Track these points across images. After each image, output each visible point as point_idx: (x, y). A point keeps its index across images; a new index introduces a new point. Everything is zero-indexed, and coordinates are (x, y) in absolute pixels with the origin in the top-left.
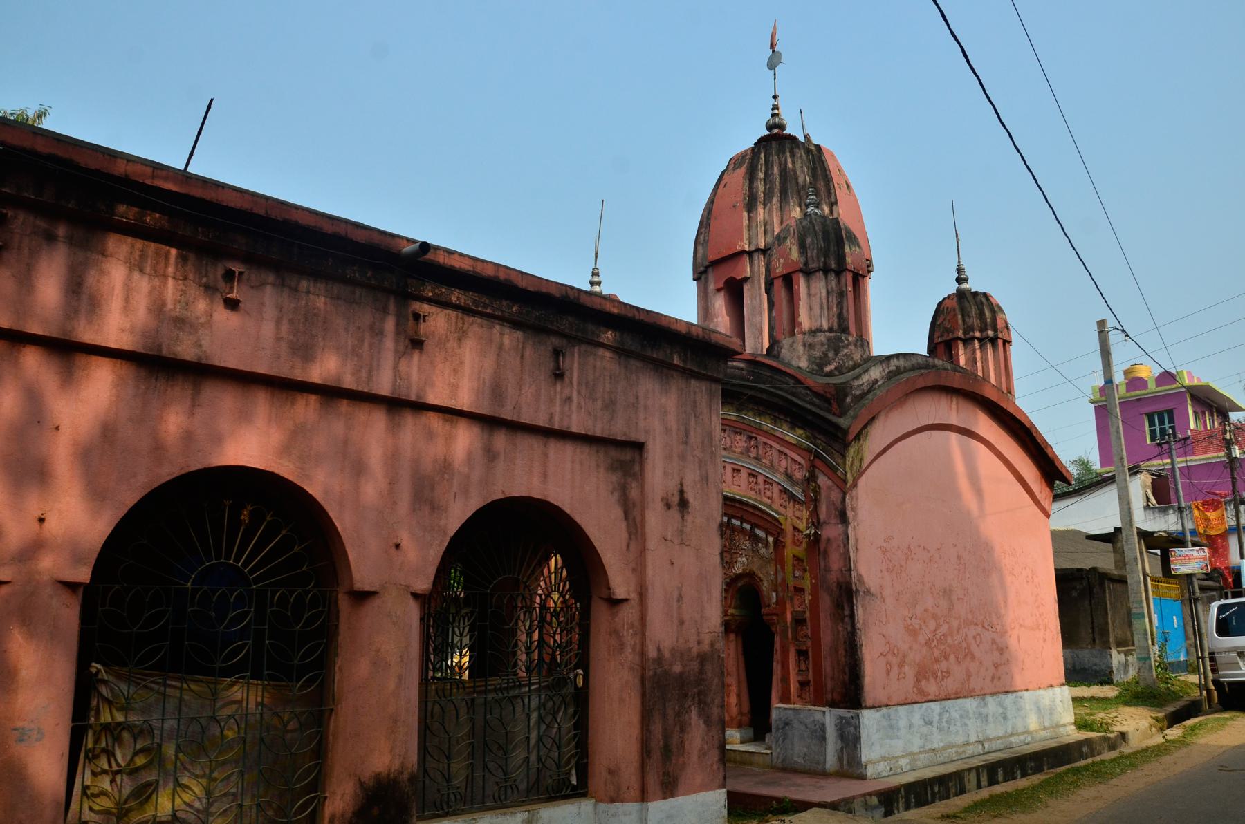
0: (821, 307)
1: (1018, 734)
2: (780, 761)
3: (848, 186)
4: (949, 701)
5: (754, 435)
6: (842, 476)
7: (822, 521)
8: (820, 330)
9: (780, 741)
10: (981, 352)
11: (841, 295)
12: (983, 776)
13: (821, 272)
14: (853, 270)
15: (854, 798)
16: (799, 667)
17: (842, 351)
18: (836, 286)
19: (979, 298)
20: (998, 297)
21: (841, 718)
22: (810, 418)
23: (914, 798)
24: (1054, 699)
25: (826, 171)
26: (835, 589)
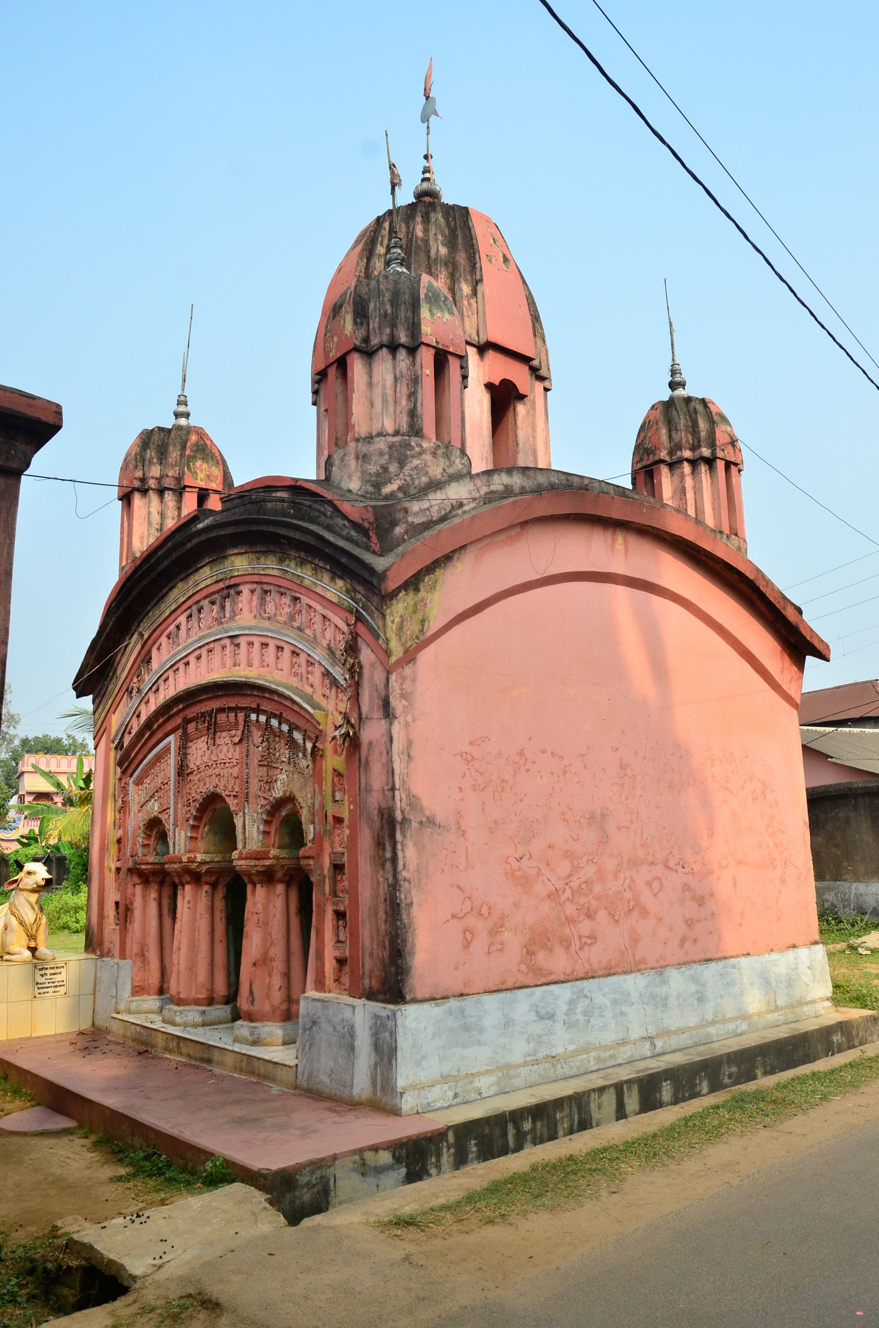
0: (385, 401)
1: (724, 1021)
2: (305, 1078)
3: (506, 260)
4: (591, 981)
5: (298, 595)
6: (384, 646)
7: (364, 716)
8: (380, 434)
9: (307, 1048)
10: (694, 479)
11: (415, 381)
12: (630, 1097)
13: (385, 350)
14: (434, 344)
15: (334, 1158)
16: (337, 935)
17: (411, 462)
18: (409, 369)
19: (692, 404)
20: (721, 403)
21: (377, 1017)
22: (343, 560)
23: (476, 1145)
24: (797, 964)
25: (472, 239)
26: (376, 818)
